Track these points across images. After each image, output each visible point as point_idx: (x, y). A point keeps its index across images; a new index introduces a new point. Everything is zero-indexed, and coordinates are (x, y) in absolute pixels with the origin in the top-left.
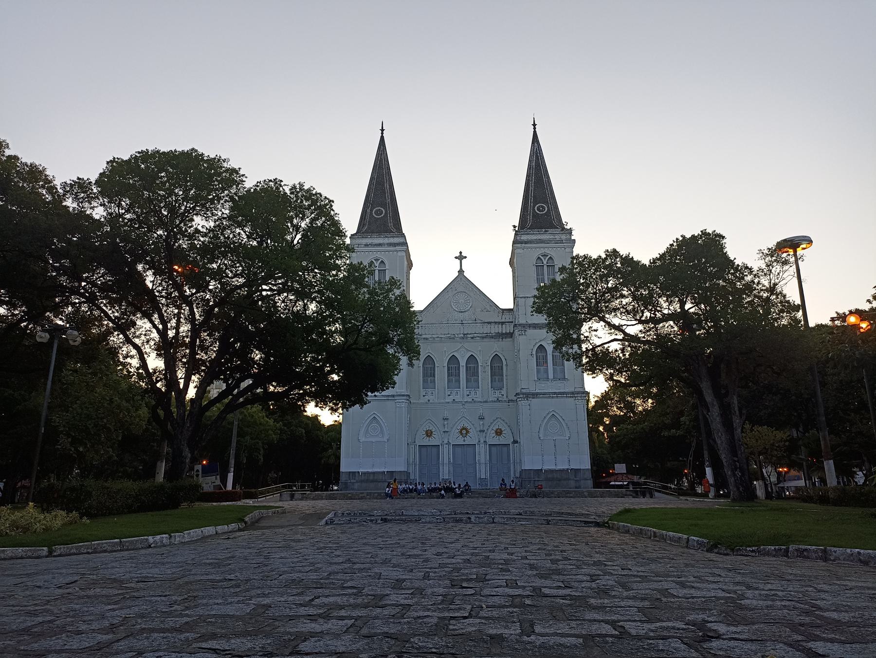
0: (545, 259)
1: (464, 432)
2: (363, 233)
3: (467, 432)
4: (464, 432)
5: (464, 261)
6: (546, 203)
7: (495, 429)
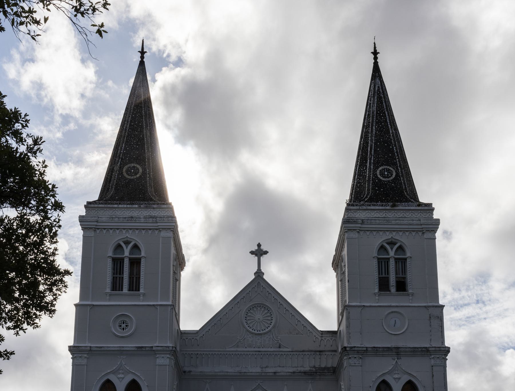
0: (392, 249)
2: (106, 200)
5: (263, 259)
6: (394, 165)
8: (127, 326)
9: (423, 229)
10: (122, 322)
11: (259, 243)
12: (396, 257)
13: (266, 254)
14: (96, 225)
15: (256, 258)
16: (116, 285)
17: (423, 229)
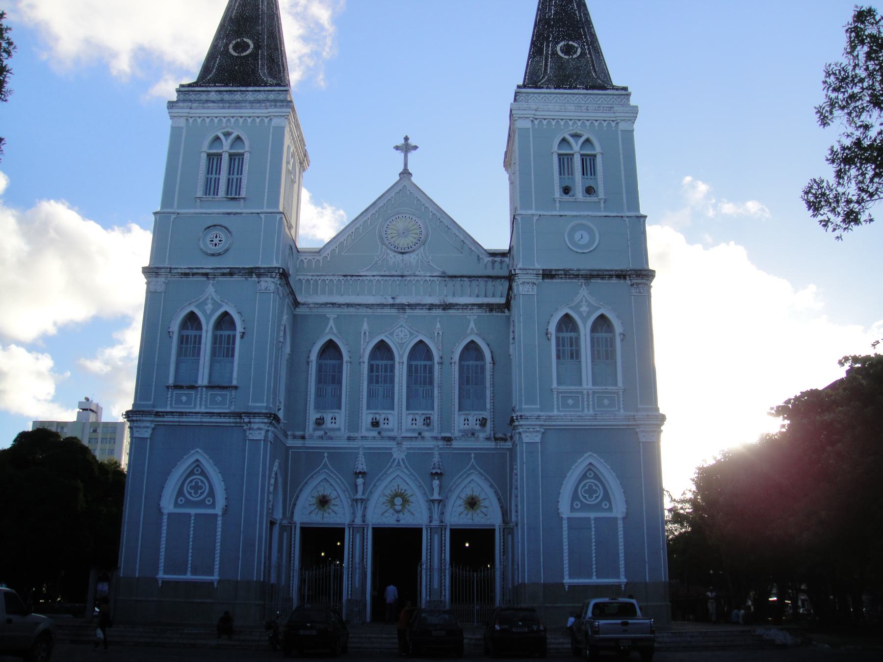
1: (398, 501)
3: (405, 501)
4: (398, 501)
5: (412, 155)
6: (578, 38)
7: (463, 496)
8: (220, 241)
9: (617, 118)
10: (215, 235)
11: (407, 136)
12: (583, 152)
13: (416, 149)
14: (189, 113)
15: (402, 155)
16: (211, 187)
17: (617, 118)
